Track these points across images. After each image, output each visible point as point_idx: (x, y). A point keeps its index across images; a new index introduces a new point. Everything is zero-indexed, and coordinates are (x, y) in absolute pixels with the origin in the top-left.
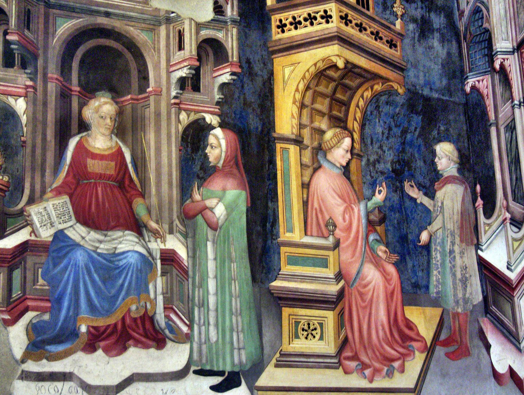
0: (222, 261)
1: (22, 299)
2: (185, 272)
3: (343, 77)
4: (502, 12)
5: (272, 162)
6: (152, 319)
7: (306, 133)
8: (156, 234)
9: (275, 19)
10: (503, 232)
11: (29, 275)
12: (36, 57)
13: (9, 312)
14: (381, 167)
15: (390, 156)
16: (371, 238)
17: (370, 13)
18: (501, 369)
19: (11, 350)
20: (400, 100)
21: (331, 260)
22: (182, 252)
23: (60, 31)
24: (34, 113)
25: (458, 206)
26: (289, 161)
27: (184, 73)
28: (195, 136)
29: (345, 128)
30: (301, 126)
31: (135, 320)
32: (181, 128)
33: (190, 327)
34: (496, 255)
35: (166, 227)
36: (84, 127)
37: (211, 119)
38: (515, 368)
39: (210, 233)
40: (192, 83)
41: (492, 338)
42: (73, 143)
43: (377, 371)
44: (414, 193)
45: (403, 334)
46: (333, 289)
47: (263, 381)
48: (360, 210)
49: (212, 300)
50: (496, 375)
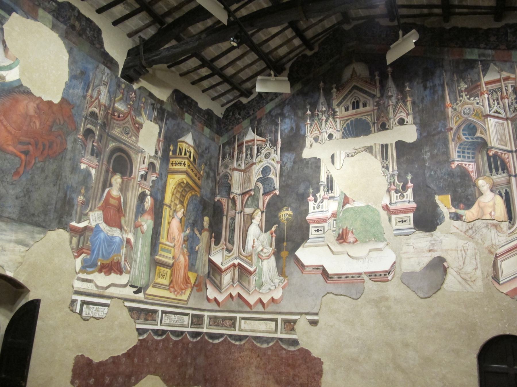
0: (143, 245)
1: (82, 249)
2: (132, 247)
3: (185, 187)
4: (238, 180)
5: (162, 212)
6: (120, 264)
7: (173, 204)
8: (126, 231)
9: (171, 160)
10: (222, 252)
11: (86, 239)
12: (101, 154)
13: (77, 253)
14: (190, 221)
15: (193, 218)
16: (184, 245)
17: (196, 166)
18: (211, 297)
19: (75, 268)
20: (198, 199)
21: (172, 252)
22: (132, 240)
23: (110, 146)
24: (97, 176)
25: (206, 240)
26: (166, 212)
27: (143, 173)
28: (142, 197)
29: (183, 205)
30: (172, 201)
31: (115, 263)
32: (139, 193)
33: (131, 268)
34: (217, 258)
35: (129, 229)
36: (111, 185)
37: (148, 192)
38: (217, 298)
39: (141, 234)
40: (144, 177)
41: (208, 286)
42: (107, 190)
43: (178, 293)
44: (197, 232)
45: (187, 280)
46: (171, 262)
47: (148, 292)
48: (182, 235)
49: (138, 260)
50: (208, 299)
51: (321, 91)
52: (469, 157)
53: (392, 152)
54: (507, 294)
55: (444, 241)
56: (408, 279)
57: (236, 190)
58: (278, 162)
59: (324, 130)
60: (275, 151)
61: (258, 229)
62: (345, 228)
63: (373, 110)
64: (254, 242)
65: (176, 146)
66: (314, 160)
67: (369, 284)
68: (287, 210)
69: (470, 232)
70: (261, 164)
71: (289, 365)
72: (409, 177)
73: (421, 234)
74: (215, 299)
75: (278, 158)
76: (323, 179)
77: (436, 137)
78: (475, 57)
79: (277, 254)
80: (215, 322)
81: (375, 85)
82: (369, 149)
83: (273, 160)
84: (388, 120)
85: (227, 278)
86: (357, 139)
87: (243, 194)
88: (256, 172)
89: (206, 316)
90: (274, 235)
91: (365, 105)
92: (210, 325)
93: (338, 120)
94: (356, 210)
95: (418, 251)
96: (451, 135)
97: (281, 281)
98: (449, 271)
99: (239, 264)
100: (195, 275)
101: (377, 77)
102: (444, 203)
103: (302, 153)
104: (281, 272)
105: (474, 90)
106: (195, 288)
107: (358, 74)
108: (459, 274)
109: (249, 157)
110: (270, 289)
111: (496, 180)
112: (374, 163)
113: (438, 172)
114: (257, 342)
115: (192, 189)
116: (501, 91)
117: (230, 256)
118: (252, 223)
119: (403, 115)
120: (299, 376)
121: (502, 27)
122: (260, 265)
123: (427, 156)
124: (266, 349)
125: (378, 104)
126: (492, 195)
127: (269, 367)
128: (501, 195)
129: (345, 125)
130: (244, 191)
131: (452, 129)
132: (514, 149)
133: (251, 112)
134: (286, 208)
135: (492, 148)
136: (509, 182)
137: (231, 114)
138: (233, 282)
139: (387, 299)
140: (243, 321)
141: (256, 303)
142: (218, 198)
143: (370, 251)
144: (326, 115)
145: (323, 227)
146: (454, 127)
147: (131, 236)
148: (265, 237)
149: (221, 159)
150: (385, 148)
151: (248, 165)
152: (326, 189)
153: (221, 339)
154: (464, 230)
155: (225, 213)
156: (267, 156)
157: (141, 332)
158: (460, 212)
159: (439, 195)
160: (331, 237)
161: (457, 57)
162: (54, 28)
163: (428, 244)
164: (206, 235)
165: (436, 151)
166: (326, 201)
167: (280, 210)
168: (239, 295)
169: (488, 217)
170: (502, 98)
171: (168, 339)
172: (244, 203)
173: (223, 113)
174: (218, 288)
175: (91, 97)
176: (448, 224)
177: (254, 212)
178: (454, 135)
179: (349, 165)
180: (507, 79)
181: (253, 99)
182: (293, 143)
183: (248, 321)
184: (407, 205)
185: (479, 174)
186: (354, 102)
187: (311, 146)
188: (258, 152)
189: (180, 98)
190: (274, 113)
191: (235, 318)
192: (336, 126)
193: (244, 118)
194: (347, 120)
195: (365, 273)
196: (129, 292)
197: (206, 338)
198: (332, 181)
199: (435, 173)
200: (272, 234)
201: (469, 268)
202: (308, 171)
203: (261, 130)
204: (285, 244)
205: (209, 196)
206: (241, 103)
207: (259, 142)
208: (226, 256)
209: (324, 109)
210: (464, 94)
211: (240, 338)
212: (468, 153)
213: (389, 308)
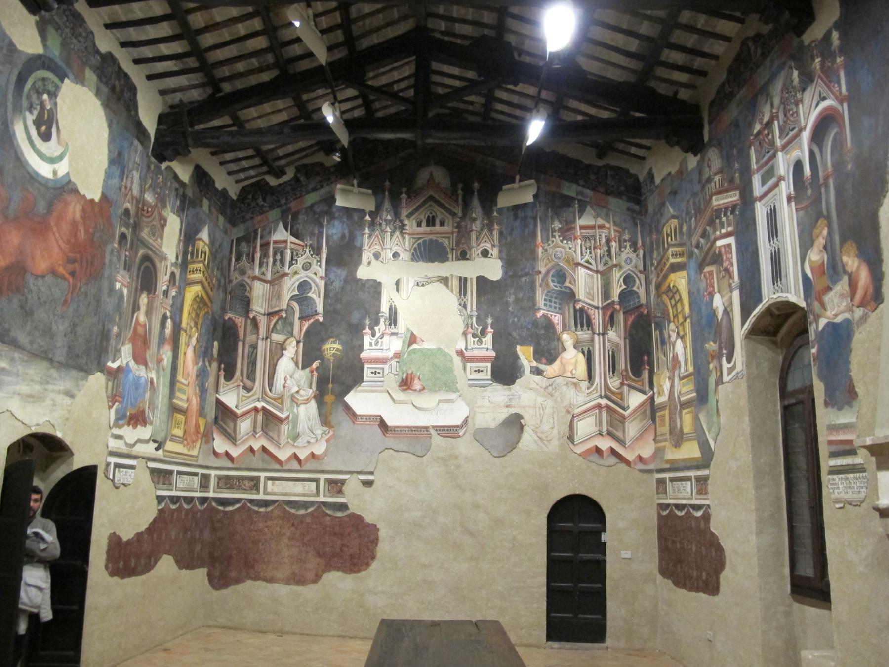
0: (164, 385)
4: (261, 294)
15: (204, 345)
20: (210, 317)
34: (230, 399)
37: (169, 314)
40: (166, 293)
41: (215, 436)
42: (136, 315)
44: (207, 364)
46: (185, 405)
48: (195, 368)
50: (216, 454)
51: (387, 193)
52: (555, 308)
53: (472, 288)
54: (580, 455)
55: (522, 397)
56: (481, 435)
57: (258, 307)
58: (321, 278)
59: (388, 246)
60: (318, 262)
61: (292, 365)
62: (410, 372)
63: (453, 233)
64: (286, 381)
65: (193, 246)
66: (372, 283)
67: (437, 440)
68: (334, 343)
69: (550, 389)
70: (297, 277)
71: (335, 534)
72: (490, 321)
73: (498, 387)
74: (227, 454)
75: (322, 272)
76: (385, 308)
77: (523, 279)
78: (572, 194)
79: (319, 398)
80: (227, 484)
81: (457, 201)
82: (445, 281)
83: (315, 274)
84: (470, 248)
85: (244, 426)
86: (430, 264)
87: (270, 315)
88: (289, 287)
89: (213, 476)
90: (315, 373)
91: (442, 224)
92: (219, 487)
93: (407, 237)
94: (427, 354)
95: (493, 404)
96: (539, 279)
97: (324, 433)
98: (526, 429)
99: (264, 408)
100: (204, 421)
101: (460, 192)
102: (525, 355)
103: (356, 271)
104: (325, 420)
105: (567, 232)
106: (204, 439)
107: (436, 181)
108: (536, 432)
109: (278, 263)
110: (309, 442)
111: (580, 337)
112: (449, 298)
113: (522, 319)
114: (291, 508)
115: (205, 304)
116: (595, 240)
117: (249, 397)
118: (283, 355)
119: (488, 246)
120: (348, 547)
121: (604, 166)
122: (295, 410)
123: (511, 299)
124: (303, 516)
125: (459, 226)
126: (575, 351)
127: (306, 538)
128: (583, 353)
129: (416, 245)
130: (271, 311)
131: (540, 272)
132: (600, 305)
133: (283, 201)
134: (332, 340)
135: (580, 301)
136: (592, 341)
137: (250, 196)
138: (254, 431)
139: (457, 457)
140: (270, 483)
141: (289, 459)
142: (228, 316)
143: (440, 401)
144: (391, 226)
145: (383, 369)
146: (543, 270)
147: (153, 375)
148: (302, 375)
149: (233, 260)
150: (463, 281)
151: (277, 275)
152: (387, 322)
153: (237, 506)
154: (544, 386)
155: (241, 337)
156: (307, 267)
157: (160, 499)
158: (542, 367)
159: (522, 345)
160: (392, 382)
161: (554, 189)
162: (98, 94)
163: (505, 399)
164: (215, 365)
165: (521, 295)
166: (386, 338)
167: (323, 341)
168: (264, 449)
169: (569, 375)
170: (595, 248)
171: (181, 507)
172: (271, 326)
173: (238, 193)
174: (232, 438)
175: (126, 188)
176: (527, 379)
177: (286, 340)
178: (543, 280)
179: (418, 294)
180: (601, 227)
181: (285, 183)
182: (344, 255)
183: (277, 482)
184: (484, 353)
185: (564, 329)
186: (428, 217)
187: (369, 263)
188: (292, 259)
189: (201, 176)
190: (318, 209)
191: (257, 479)
192: (404, 244)
193: (271, 207)
194: (419, 238)
195: (433, 427)
196: (149, 449)
197: (214, 504)
198: (396, 313)
199: (519, 320)
200: (312, 372)
201: (546, 427)
202: (364, 296)
203: (298, 230)
204: (330, 386)
205: (219, 312)
206: (267, 183)
207: (293, 246)
208: (243, 396)
209: (389, 218)
210: (557, 234)
211: (266, 503)
212: (555, 303)
213: (458, 467)
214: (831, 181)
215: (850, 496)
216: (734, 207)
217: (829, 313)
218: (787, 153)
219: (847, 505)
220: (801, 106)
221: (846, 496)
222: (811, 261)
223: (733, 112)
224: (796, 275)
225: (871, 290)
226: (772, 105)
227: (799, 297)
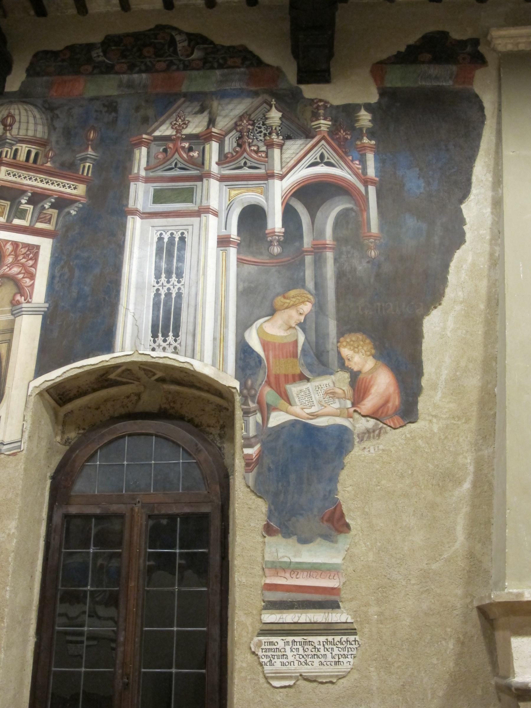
214: (330, 255)
215: (314, 668)
216: (62, 203)
217: (296, 409)
218: (231, 187)
219: (301, 682)
220: (277, 152)
221: (304, 669)
222: (261, 332)
223: (108, 86)
224: (219, 341)
225: (396, 401)
226: (212, 122)
227: (224, 370)
